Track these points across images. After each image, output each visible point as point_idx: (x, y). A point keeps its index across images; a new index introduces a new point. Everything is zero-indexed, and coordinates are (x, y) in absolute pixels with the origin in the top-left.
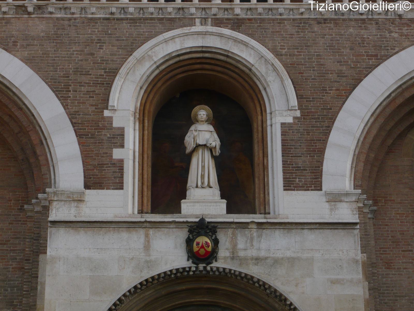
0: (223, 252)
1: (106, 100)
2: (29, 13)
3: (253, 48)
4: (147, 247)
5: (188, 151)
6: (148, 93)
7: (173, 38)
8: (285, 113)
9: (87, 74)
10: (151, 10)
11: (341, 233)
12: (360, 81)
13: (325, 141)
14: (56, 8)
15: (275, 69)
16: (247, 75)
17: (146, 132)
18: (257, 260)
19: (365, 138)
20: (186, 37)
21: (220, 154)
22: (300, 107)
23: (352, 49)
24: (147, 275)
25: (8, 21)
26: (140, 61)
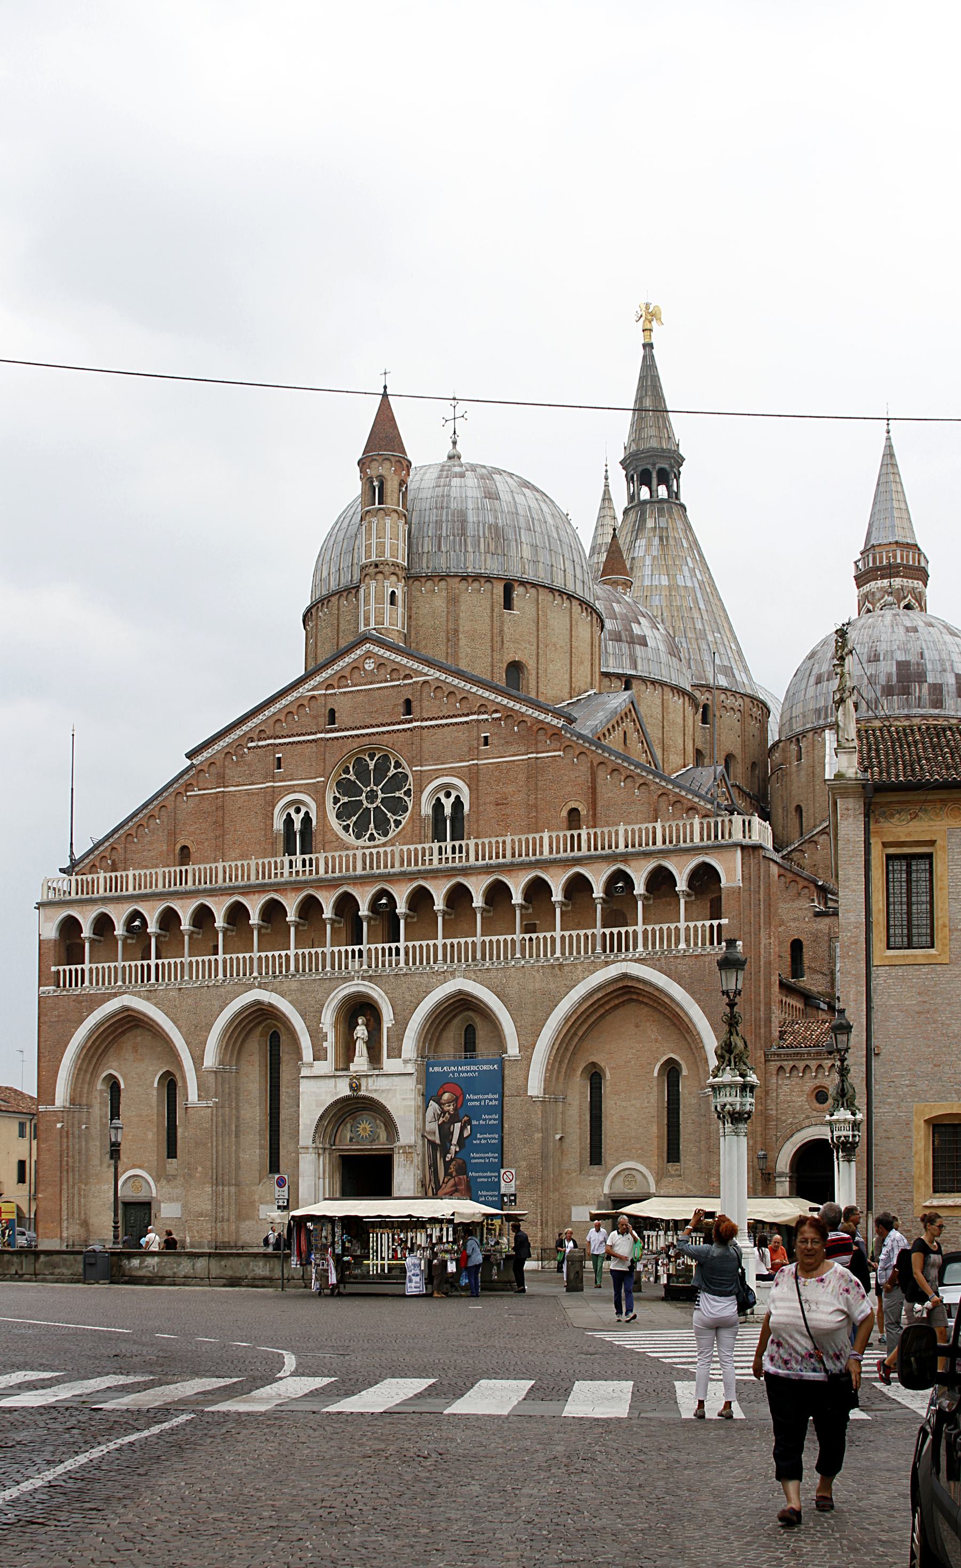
0: (363, 1088)
4: (335, 1086)
11: (407, 1077)
18: (376, 1090)
24: (335, 1099)
26: (332, 999)
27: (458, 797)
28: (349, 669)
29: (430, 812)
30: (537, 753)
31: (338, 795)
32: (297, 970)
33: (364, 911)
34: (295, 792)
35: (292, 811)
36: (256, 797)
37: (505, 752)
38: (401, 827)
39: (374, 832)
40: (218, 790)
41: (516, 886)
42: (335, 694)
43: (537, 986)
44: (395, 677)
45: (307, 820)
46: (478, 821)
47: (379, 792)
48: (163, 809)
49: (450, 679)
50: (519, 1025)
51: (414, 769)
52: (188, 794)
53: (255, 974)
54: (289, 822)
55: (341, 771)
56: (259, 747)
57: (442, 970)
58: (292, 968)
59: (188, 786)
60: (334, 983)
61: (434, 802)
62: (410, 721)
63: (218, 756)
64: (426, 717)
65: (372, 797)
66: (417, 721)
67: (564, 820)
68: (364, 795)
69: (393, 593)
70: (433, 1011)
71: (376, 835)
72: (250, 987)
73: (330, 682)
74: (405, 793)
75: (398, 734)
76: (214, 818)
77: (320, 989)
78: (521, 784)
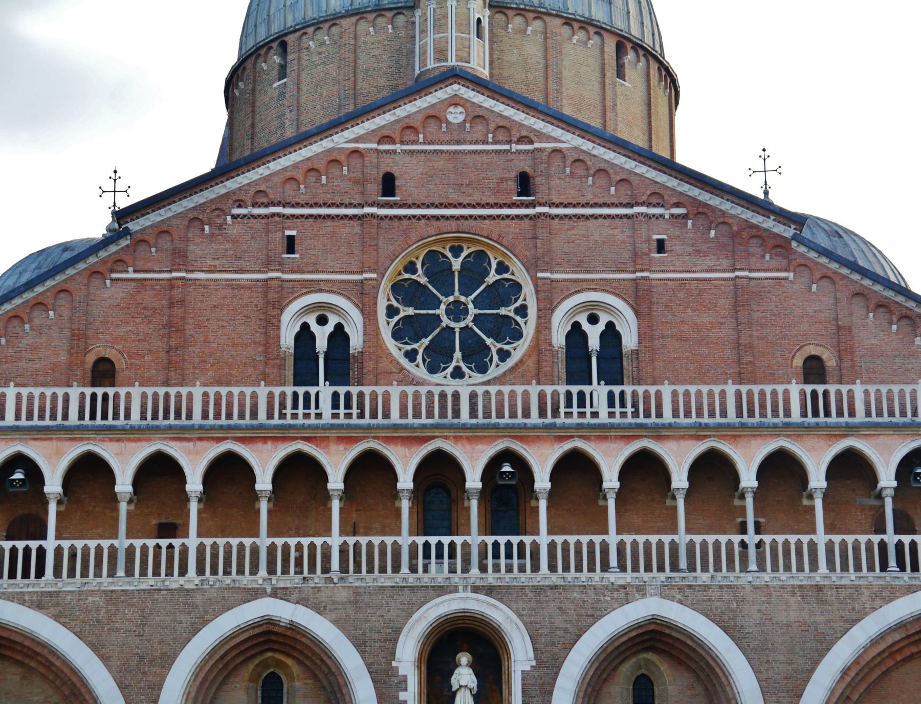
1: (393, 654)
2: (335, 583)
3: (501, 610)
5: (454, 689)
6: (424, 644)
7: (442, 602)
8: (525, 663)
9: (379, 632)
10: (426, 580)
12: (581, 636)
13: (553, 685)
14: (354, 579)
15: (518, 627)
16: (497, 630)
17: (423, 675)
19: (584, 679)
20: (451, 602)
21: (477, 692)
22: (536, 658)
23: (575, 610)
25: (319, 589)
27: (610, 326)
28: (420, 117)
29: (563, 341)
30: (751, 271)
31: (395, 304)
32: (344, 569)
33: (474, 481)
34: (320, 291)
35: (311, 320)
36: (247, 294)
37: (695, 265)
38: (510, 362)
39: (462, 364)
40: (175, 274)
41: (749, 461)
42: (395, 152)
43: (793, 616)
44: (500, 138)
45: (339, 336)
46: (653, 361)
47: (471, 306)
48: (62, 295)
49: (600, 151)
50: (764, 676)
51: (540, 275)
52: (114, 276)
53: (263, 572)
54: (305, 336)
55: (401, 268)
56: (253, 216)
57: (622, 582)
58: (335, 564)
59: (118, 263)
60: (420, 595)
61: (569, 328)
62: (532, 205)
63: (174, 222)
64: (557, 201)
65: (457, 311)
66: (544, 205)
67: (801, 371)
68: (443, 307)
69: (479, 20)
70: (603, 649)
71: (465, 369)
72: (254, 594)
73: (386, 133)
74: (517, 311)
75: (508, 222)
76: (165, 319)
77: (393, 603)
78: (722, 313)
